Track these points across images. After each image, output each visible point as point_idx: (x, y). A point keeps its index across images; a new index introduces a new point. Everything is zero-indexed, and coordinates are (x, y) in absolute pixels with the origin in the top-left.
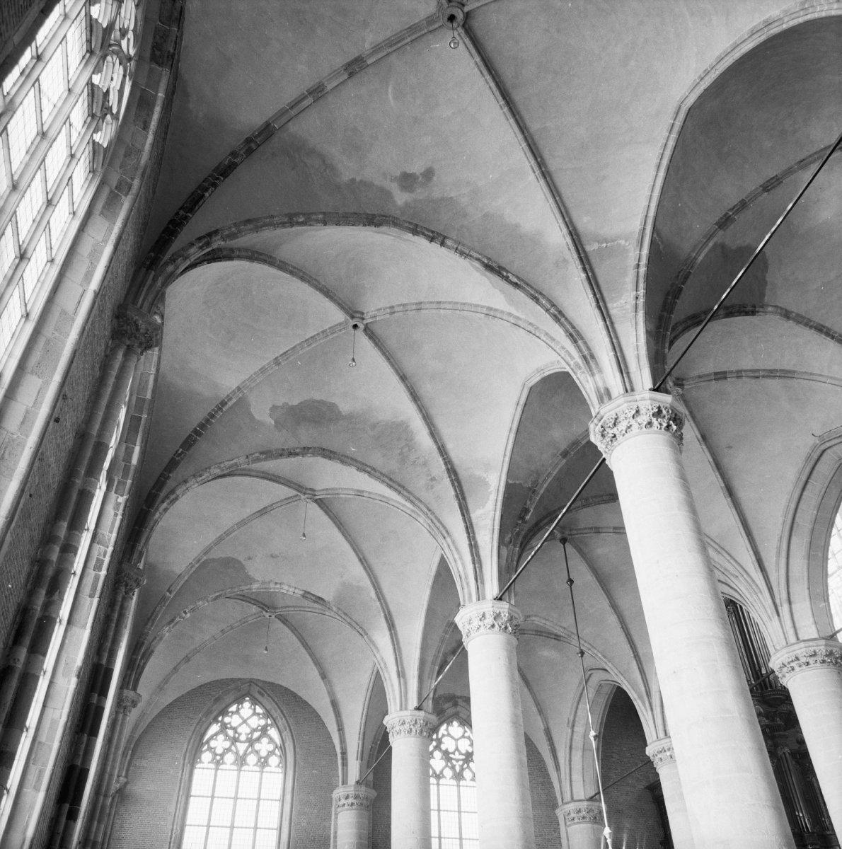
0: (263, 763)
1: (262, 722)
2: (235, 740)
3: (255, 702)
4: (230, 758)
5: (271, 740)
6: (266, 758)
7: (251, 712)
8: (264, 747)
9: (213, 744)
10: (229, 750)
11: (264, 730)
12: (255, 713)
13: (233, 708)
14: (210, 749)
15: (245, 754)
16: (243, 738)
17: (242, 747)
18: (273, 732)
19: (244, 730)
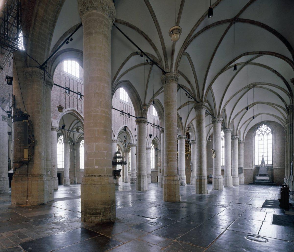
0: (268, 134)
1: (267, 128)
2: (262, 132)
3: (265, 125)
4: (261, 135)
5: (269, 130)
6: (269, 133)
7: (264, 127)
8: (268, 132)
9: (257, 133)
10: (261, 133)
11: (267, 129)
12: (265, 127)
13: (261, 127)
14: (257, 134)
15: (264, 134)
16: (263, 131)
17: (263, 133)
18: (269, 129)
19: (263, 130)
